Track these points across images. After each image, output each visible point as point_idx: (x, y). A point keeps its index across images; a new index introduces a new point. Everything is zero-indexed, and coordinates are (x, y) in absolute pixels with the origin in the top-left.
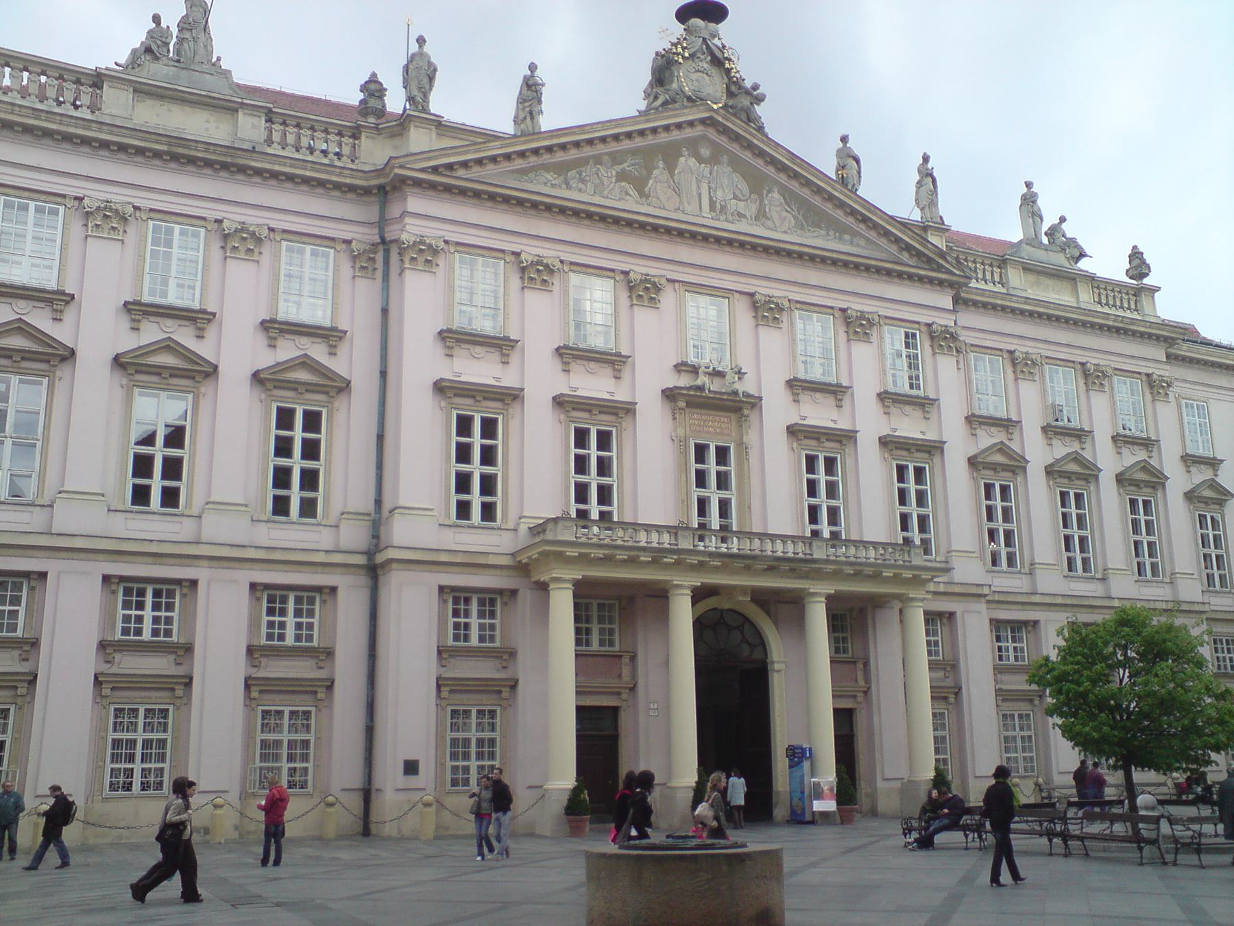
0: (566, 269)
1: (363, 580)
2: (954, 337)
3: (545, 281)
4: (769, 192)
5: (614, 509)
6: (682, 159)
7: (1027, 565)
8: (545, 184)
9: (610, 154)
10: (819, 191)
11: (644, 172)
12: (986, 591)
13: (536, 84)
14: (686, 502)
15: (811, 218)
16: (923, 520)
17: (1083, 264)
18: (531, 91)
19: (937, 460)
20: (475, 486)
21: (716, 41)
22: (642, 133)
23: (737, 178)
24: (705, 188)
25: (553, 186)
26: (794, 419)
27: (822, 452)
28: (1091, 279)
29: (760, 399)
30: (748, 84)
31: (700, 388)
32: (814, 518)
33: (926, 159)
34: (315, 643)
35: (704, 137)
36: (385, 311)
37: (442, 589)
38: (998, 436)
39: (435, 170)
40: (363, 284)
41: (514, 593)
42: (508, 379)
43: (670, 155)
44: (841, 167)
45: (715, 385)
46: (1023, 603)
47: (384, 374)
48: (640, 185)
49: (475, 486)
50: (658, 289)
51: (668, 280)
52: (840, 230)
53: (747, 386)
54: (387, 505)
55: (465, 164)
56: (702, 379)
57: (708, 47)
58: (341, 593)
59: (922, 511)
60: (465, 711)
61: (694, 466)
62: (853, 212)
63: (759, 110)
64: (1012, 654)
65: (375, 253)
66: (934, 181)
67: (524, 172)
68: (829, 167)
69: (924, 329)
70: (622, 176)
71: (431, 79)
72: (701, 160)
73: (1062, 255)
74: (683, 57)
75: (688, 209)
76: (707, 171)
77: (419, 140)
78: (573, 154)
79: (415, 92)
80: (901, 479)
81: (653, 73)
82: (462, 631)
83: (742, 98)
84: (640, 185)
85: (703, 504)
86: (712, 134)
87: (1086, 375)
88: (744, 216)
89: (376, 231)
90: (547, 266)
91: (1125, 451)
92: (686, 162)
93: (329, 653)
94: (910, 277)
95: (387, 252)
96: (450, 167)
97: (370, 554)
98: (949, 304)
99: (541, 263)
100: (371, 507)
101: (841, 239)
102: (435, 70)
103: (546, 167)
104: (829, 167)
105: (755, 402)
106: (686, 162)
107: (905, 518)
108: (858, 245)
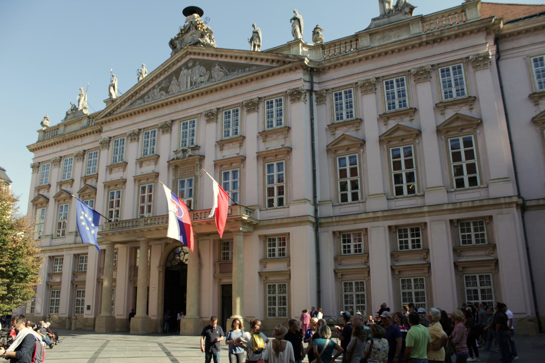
6: (182, 72)
11: (168, 84)
24: (189, 78)
35: (191, 59)
39: (103, 117)
43: (177, 73)
48: (166, 90)
67: (132, 104)
72: (188, 68)
75: (182, 90)
78: (146, 90)
84: (166, 90)
86: (193, 57)
88: (203, 82)
92: (184, 71)
103: (139, 99)
106: (184, 71)
108: (252, 70)
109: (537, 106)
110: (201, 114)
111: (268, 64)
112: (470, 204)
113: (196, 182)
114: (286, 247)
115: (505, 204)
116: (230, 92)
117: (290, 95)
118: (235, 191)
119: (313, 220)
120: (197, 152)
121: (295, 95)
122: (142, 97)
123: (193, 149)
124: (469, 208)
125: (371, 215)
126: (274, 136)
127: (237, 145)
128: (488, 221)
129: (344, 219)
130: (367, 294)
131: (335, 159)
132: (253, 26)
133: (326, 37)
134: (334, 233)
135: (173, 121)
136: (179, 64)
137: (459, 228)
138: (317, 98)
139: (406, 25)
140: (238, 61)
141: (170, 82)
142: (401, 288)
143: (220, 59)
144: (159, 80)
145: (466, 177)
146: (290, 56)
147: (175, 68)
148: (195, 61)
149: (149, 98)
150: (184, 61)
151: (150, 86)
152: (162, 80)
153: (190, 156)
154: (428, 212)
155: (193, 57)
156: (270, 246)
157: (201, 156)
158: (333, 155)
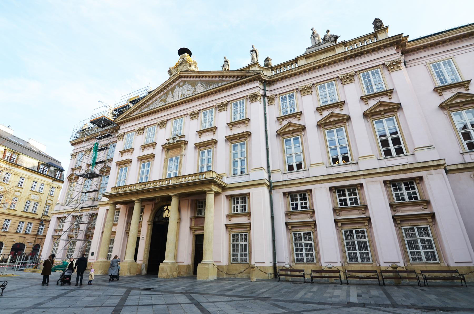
35: (182, 81)
48: (164, 101)
52: (217, 82)
72: (180, 86)
78: (151, 102)
86: (183, 79)
92: (177, 88)
103: (145, 108)
106: (177, 88)
109: (441, 97)
110: (187, 114)
111: (235, 79)
112: (401, 168)
113: (181, 159)
114: (247, 204)
115: (434, 166)
117: (249, 98)
118: (209, 164)
119: (268, 183)
120: (182, 139)
121: (253, 97)
123: (181, 137)
124: (400, 170)
125: (314, 179)
126: (238, 126)
127: (212, 133)
128: (418, 182)
129: (292, 182)
130: (314, 243)
131: (283, 141)
132: (224, 58)
133: (273, 63)
134: (284, 194)
135: (167, 120)
136: (174, 84)
137: (392, 188)
138: (269, 101)
139: (333, 49)
141: (167, 96)
142: (344, 238)
145: (392, 148)
148: (185, 82)
149: (152, 106)
150: (177, 82)
151: (154, 99)
153: (178, 141)
154: (364, 175)
156: (234, 204)
157: (186, 141)
158: (281, 138)
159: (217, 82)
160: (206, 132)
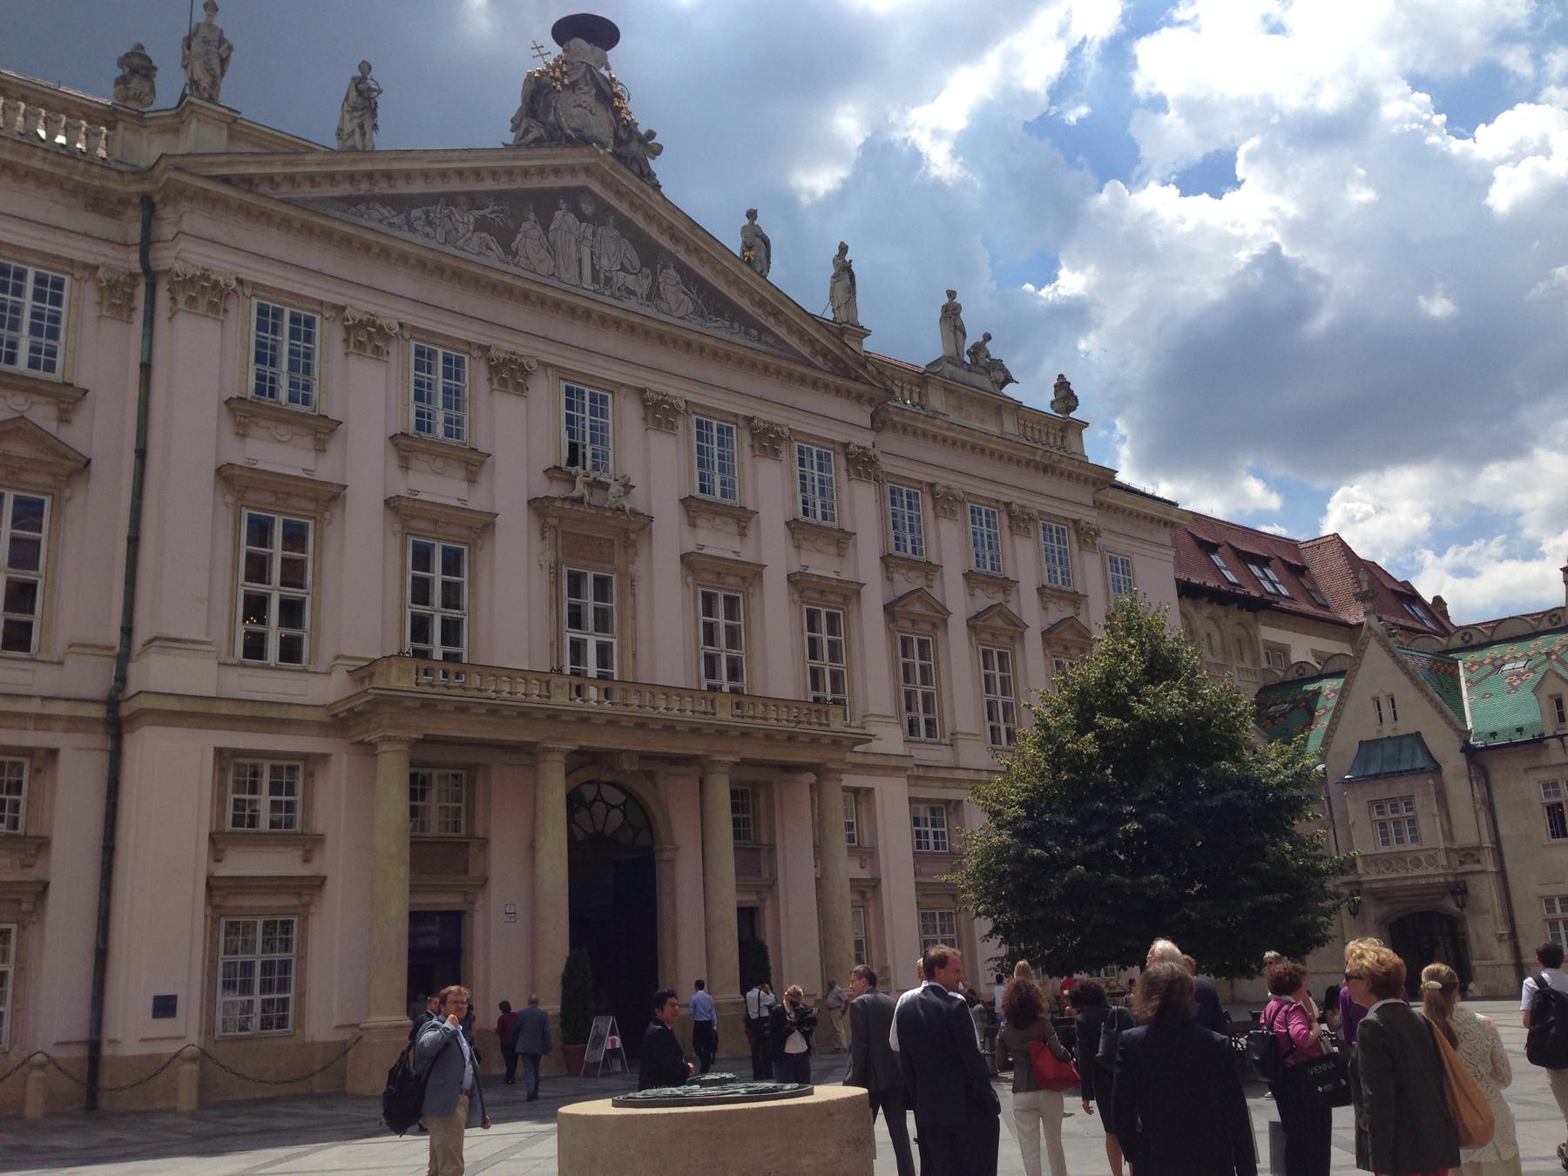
0: (407, 335)
1: (99, 740)
2: (873, 461)
3: (378, 347)
4: (664, 267)
5: (464, 650)
6: (558, 214)
7: (948, 734)
8: (381, 221)
9: (468, 194)
10: (724, 273)
12: (907, 763)
13: (370, 89)
14: (557, 644)
15: (713, 303)
16: (836, 677)
17: (1009, 390)
18: (363, 99)
19: (853, 607)
20: (273, 615)
21: (602, 71)
22: (509, 172)
23: (626, 245)
24: (586, 251)
25: (391, 225)
26: (691, 548)
27: (722, 593)
28: (1017, 407)
29: (651, 519)
30: (642, 130)
31: (579, 501)
32: (711, 671)
33: (843, 249)
34: (20, 831)
35: (585, 190)
36: (146, 368)
37: (219, 752)
38: (917, 582)
39: (226, 180)
40: (112, 328)
41: (325, 757)
42: (326, 470)
44: (747, 246)
45: (597, 498)
46: (944, 780)
47: (141, 454)
49: (273, 615)
50: (525, 372)
51: (540, 363)
53: (636, 501)
54: (142, 633)
55: (270, 179)
56: (580, 489)
57: (593, 75)
58: (63, 758)
59: (836, 666)
60: (246, 924)
61: (566, 600)
62: (762, 303)
63: (655, 165)
64: (931, 840)
65: (134, 287)
66: (852, 277)
68: (735, 246)
69: (839, 449)
70: (482, 225)
71: (224, 61)
72: (582, 218)
73: (986, 378)
74: (563, 85)
75: (566, 276)
76: (590, 230)
77: (201, 137)
79: (199, 73)
80: (812, 627)
81: (524, 99)
82: (245, 817)
83: (634, 149)
85: (577, 648)
87: (1011, 516)
89: (136, 257)
90: (380, 329)
91: (1051, 606)
93: (43, 844)
94: (826, 387)
95: (152, 289)
96: (248, 182)
97: (112, 702)
98: (867, 421)
99: (373, 324)
100: (114, 637)
101: (747, 333)
102: (230, 48)
104: (735, 246)
105: (645, 522)
107: (815, 674)
108: (766, 343)
116: (714, 372)
122: (400, 203)
140: (732, 294)
143: (692, 262)
144: (473, 186)
146: (870, 367)
147: (535, 183)
152: (488, 194)
155: (596, 188)
159: (747, 322)
160: (716, 513)
